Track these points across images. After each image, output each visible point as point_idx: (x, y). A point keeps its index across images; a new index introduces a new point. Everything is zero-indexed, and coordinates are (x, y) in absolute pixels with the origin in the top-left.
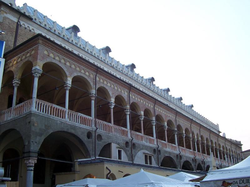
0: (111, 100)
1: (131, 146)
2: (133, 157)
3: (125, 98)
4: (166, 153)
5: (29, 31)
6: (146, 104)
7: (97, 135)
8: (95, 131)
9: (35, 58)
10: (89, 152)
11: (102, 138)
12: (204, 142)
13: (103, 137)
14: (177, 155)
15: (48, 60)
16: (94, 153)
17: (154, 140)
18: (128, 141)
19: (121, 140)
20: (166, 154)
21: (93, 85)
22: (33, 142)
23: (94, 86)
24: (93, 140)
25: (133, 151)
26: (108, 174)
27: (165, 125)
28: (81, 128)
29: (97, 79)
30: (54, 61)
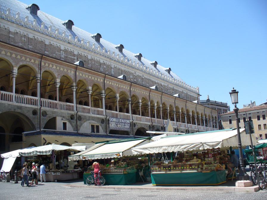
0: (56, 81)
3: (71, 77)
7: (41, 111)
8: (40, 109)
13: (48, 113)
17: (102, 112)
18: (74, 115)
21: (39, 70)
23: (39, 71)
24: (38, 116)
28: (26, 107)
29: (43, 64)
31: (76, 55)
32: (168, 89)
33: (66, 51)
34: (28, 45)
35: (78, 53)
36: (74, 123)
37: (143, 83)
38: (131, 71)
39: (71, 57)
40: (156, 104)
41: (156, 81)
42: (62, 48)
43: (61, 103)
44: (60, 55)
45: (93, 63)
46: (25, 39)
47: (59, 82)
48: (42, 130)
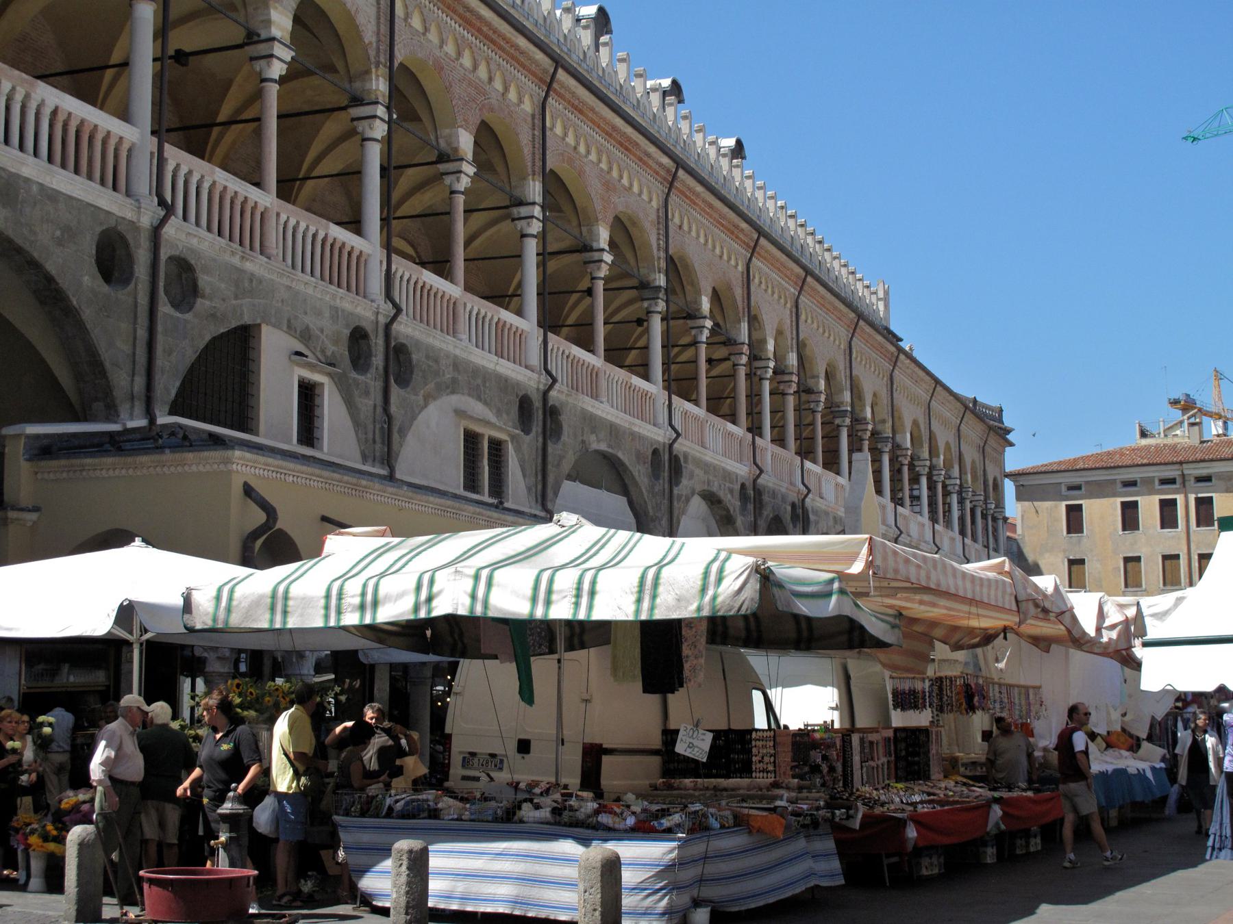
0: (268, 23)
1: (382, 362)
2: (395, 436)
4: (593, 430)
6: (491, 79)
7: (164, 256)
8: (156, 231)
10: (103, 373)
11: (201, 283)
12: (811, 383)
13: (204, 280)
14: (655, 452)
16: (140, 382)
17: (520, 335)
18: (369, 328)
19: (319, 314)
20: (593, 438)
25: (394, 399)
26: (255, 535)
27: (595, 245)
28: (53, 196)
36: (367, 393)
43: (292, 215)
48: (163, 419)
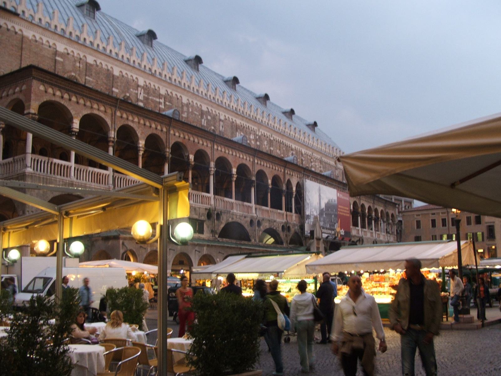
0: (139, 143)
5: (14, 34)
9: (28, 93)
15: (45, 99)
17: (209, 198)
22: (28, 211)
30: (53, 99)
31: (162, 95)
32: (312, 160)
33: (146, 89)
34: (86, 75)
35: (166, 93)
37: (272, 149)
38: (253, 127)
39: (155, 99)
40: (294, 189)
41: (293, 147)
42: (141, 82)
44: (137, 94)
45: (190, 110)
46: (81, 66)
47: (143, 147)
